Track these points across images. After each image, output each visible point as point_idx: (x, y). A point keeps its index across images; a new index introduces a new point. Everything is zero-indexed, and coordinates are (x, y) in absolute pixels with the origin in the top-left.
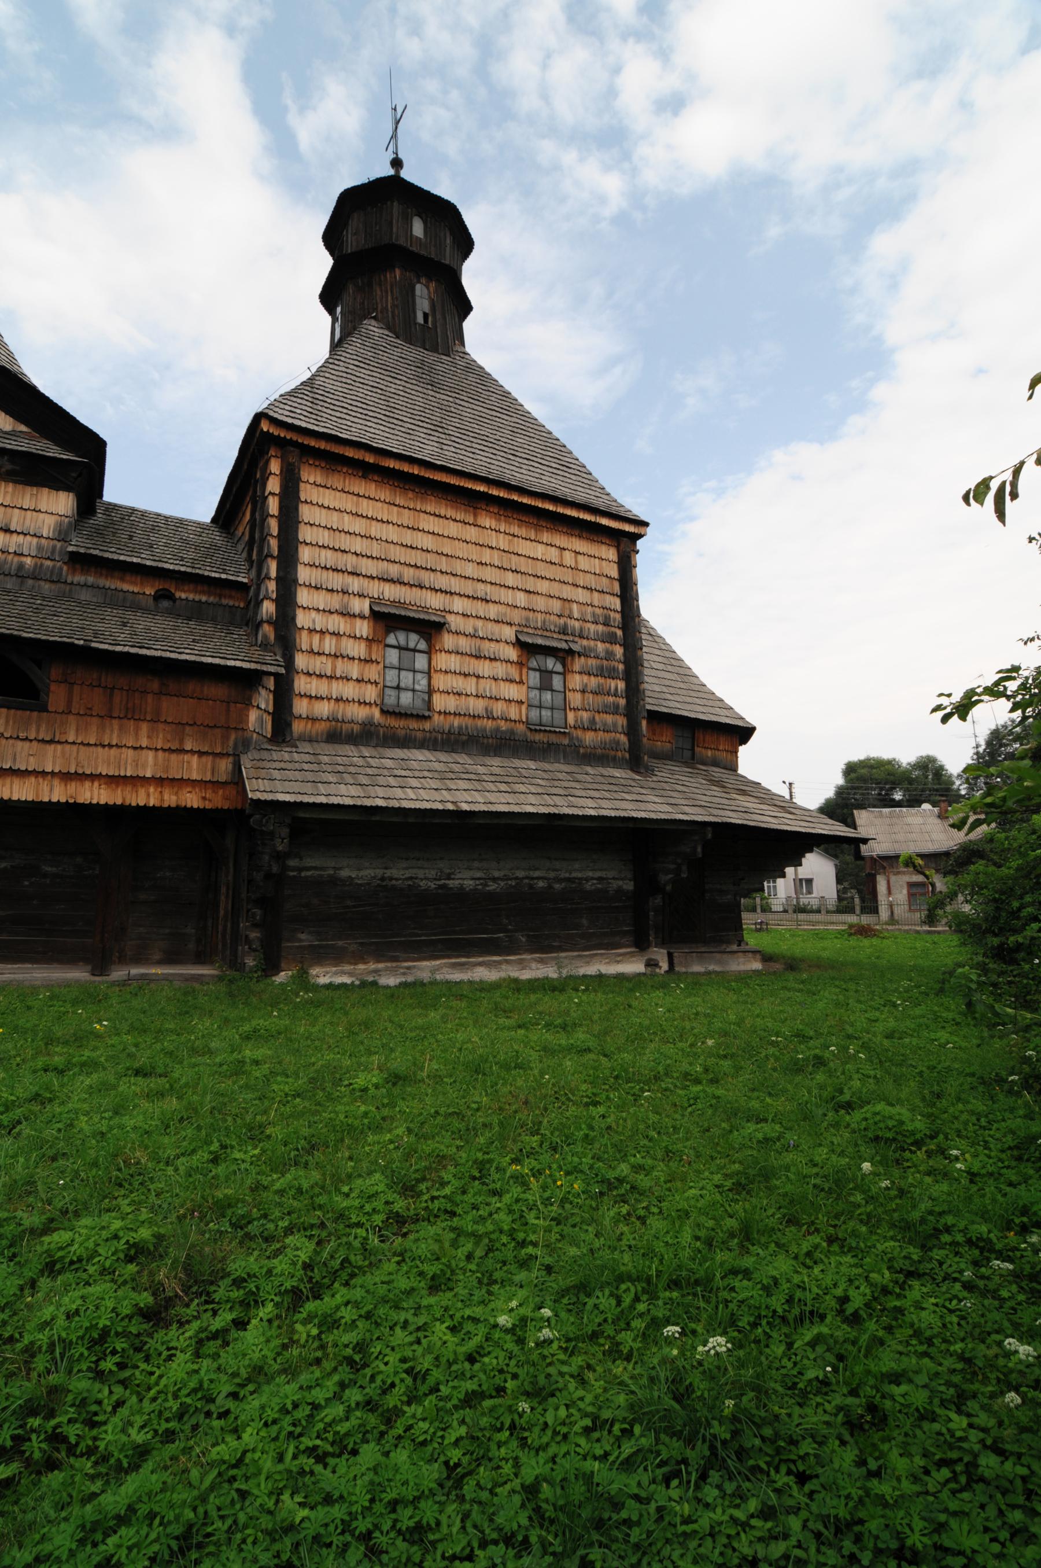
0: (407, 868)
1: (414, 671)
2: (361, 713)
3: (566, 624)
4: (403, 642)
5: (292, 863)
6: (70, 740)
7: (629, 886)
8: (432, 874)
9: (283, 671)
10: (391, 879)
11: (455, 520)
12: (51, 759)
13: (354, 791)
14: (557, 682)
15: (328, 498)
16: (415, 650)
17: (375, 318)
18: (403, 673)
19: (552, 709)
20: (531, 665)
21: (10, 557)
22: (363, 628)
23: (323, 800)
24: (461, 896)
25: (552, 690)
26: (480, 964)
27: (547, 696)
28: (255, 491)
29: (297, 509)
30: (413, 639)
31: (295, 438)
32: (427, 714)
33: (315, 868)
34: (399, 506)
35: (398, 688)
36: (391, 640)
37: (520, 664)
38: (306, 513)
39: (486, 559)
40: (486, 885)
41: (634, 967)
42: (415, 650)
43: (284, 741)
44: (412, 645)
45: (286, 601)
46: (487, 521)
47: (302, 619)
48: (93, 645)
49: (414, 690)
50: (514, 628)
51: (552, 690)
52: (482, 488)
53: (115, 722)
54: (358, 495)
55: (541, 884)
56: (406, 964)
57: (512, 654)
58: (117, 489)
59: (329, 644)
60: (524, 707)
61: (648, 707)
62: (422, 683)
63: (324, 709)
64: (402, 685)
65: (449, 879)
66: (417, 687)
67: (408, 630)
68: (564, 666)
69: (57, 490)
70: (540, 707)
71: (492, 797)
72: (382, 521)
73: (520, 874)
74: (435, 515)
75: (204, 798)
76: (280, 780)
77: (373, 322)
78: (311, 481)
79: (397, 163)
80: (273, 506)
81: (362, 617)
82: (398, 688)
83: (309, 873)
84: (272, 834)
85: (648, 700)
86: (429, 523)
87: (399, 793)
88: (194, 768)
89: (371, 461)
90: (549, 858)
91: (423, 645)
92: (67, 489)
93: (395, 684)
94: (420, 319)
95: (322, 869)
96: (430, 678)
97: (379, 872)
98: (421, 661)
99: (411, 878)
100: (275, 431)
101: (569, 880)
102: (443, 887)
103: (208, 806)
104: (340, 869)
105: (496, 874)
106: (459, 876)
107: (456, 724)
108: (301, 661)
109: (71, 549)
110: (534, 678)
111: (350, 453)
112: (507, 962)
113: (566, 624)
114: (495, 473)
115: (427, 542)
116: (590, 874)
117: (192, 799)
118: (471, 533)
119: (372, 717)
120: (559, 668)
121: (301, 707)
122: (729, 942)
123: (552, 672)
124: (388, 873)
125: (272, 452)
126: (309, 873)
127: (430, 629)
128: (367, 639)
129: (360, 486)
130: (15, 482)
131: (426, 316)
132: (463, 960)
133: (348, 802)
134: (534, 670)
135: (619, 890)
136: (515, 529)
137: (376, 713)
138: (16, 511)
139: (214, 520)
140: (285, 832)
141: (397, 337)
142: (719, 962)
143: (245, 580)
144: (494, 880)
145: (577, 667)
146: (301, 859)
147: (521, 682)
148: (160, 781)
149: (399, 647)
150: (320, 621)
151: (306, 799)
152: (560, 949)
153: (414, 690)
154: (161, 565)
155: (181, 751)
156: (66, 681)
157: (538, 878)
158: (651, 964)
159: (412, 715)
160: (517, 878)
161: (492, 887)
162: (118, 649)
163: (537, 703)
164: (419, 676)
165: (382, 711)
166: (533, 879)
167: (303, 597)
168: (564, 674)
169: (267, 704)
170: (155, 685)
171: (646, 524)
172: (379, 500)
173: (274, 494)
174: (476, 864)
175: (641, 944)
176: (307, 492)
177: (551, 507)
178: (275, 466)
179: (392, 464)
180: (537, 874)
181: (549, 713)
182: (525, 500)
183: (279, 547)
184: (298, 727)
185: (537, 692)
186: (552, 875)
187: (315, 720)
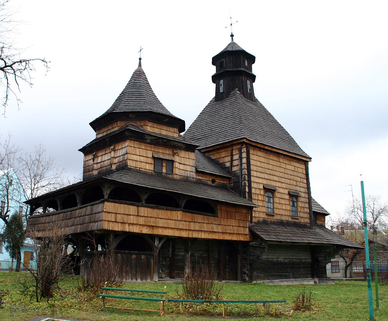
7: (310, 261)
8: (275, 257)
12: (220, 229)
22: (262, 192)
24: (281, 263)
25: (295, 207)
26: (285, 281)
27: (294, 208)
32: (273, 214)
40: (285, 260)
41: (312, 283)
46: (281, 160)
51: (295, 207)
52: (282, 152)
53: (229, 219)
56: (273, 281)
61: (313, 210)
64: (269, 207)
66: (271, 207)
67: (269, 192)
68: (297, 200)
71: (309, 239)
73: (291, 257)
75: (244, 238)
79: (232, 36)
85: (313, 208)
96: (273, 205)
99: (272, 258)
100: (247, 142)
101: (299, 259)
102: (277, 261)
105: (287, 257)
112: (290, 281)
115: (271, 167)
116: (303, 257)
117: (242, 238)
118: (278, 164)
122: (324, 278)
125: (244, 146)
131: (250, 89)
135: (309, 262)
136: (286, 162)
142: (326, 282)
144: (286, 259)
152: (298, 278)
157: (294, 259)
158: (315, 282)
161: (286, 261)
166: (293, 259)
171: (311, 158)
174: (283, 255)
175: (313, 277)
176: (252, 157)
179: (266, 148)
180: (294, 257)
182: (290, 155)
183: (247, 172)
186: (296, 258)
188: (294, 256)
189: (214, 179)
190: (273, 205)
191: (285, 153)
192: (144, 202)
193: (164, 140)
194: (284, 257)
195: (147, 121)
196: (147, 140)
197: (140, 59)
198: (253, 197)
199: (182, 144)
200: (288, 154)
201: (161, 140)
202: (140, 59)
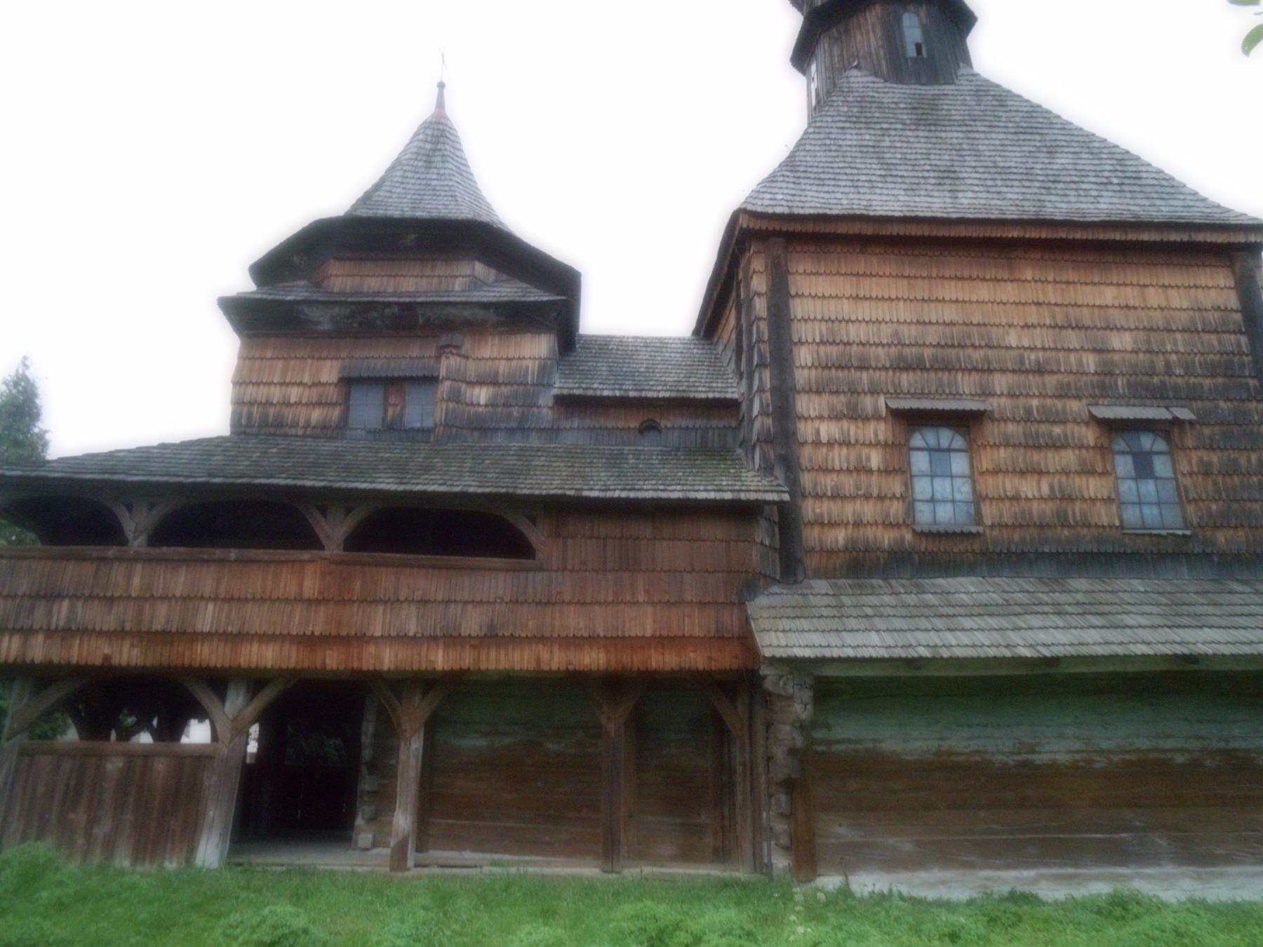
0: (969, 739)
1: (952, 477)
2: (887, 538)
3: (1163, 383)
4: (932, 442)
5: (819, 734)
6: (567, 600)
9: (786, 497)
10: (950, 754)
11: (984, 280)
13: (889, 639)
14: (1162, 466)
15: (824, 285)
16: (949, 450)
17: (857, 67)
18: (938, 483)
19: (1159, 504)
20: (1116, 448)
21: (500, 409)
22: (881, 430)
23: (850, 653)
25: (1156, 478)
27: (1149, 487)
28: (738, 295)
29: (787, 305)
30: (946, 437)
31: (777, 228)
32: (974, 529)
33: (849, 741)
34: (909, 277)
35: (932, 500)
36: (917, 440)
37: (1104, 450)
38: (799, 308)
39: (1033, 319)
42: (949, 450)
43: (795, 582)
44: (944, 443)
45: (783, 412)
47: (805, 430)
48: (585, 493)
49: (953, 501)
50: (1084, 401)
52: (1015, 233)
54: (858, 275)
55: (1180, 759)
57: (1090, 435)
58: (596, 318)
59: (839, 457)
60: (1114, 507)
62: (964, 490)
63: (839, 537)
64: (938, 496)
65: (1033, 751)
66: (958, 497)
69: (539, 333)
70: (1140, 503)
72: (890, 299)
73: (1145, 744)
74: (956, 278)
75: (710, 658)
76: (798, 630)
77: (855, 72)
78: (801, 270)
80: (760, 307)
81: (877, 417)
82: (932, 500)
83: (841, 747)
84: (790, 698)
86: (950, 290)
87: (950, 638)
88: (696, 623)
89: (870, 232)
90: (1187, 719)
91: (959, 442)
92: (547, 330)
93: (928, 496)
94: (911, 52)
95: (857, 741)
97: (933, 745)
98: (959, 464)
99: (978, 752)
103: (714, 666)
104: (880, 741)
105: (1105, 745)
106: (1047, 748)
107: (1017, 536)
108: (806, 480)
109: (555, 391)
110: (1124, 465)
111: (842, 229)
113: (1163, 383)
114: (1030, 210)
117: (696, 659)
119: (903, 539)
120: (1161, 445)
121: (812, 536)
123: (1151, 453)
124: (945, 745)
126: (841, 747)
127: (965, 422)
128: (886, 445)
129: (860, 263)
130: (501, 333)
131: (918, 47)
132: (1070, 870)
133: (884, 653)
134: (1123, 453)
137: (908, 536)
138: (503, 362)
139: (696, 332)
140: (807, 695)
141: (886, 81)
143: (736, 396)
144: (1101, 752)
145: (1190, 442)
146: (829, 727)
147: (1105, 473)
148: (661, 641)
149: (930, 450)
150: (828, 430)
151: (828, 653)
153: (953, 501)
154: (643, 394)
155: (680, 603)
156: (559, 536)
159: (955, 534)
160: (1138, 751)
162: (609, 494)
163: (1135, 499)
164: (958, 482)
165: (914, 531)
166: (1164, 751)
167: (805, 404)
168: (1171, 453)
169: (772, 537)
170: (646, 530)
172: (884, 275)
173: (760, 294)
174: (1071, 731)
177: (1118, 236)
178: (758, 264)
180: (1170, 744)
181: (1155, 510)
184: (812, 562)
185: (1132, 484)
186: (1195, 745)
187: (831, 552)
188: (1169, 737)
189: (649, 420)
190: (974, 482)
191: (1033, 234)
192: (138, 543)
193: (387, 311)
194: (1078, 745)
195: (332, 261)
196: (318, 323)
197: (441, 86)
198: (806, 455)
199: (481, 313)
200: (1078, 236)
201: (376, 314)
202: (441, 86)
